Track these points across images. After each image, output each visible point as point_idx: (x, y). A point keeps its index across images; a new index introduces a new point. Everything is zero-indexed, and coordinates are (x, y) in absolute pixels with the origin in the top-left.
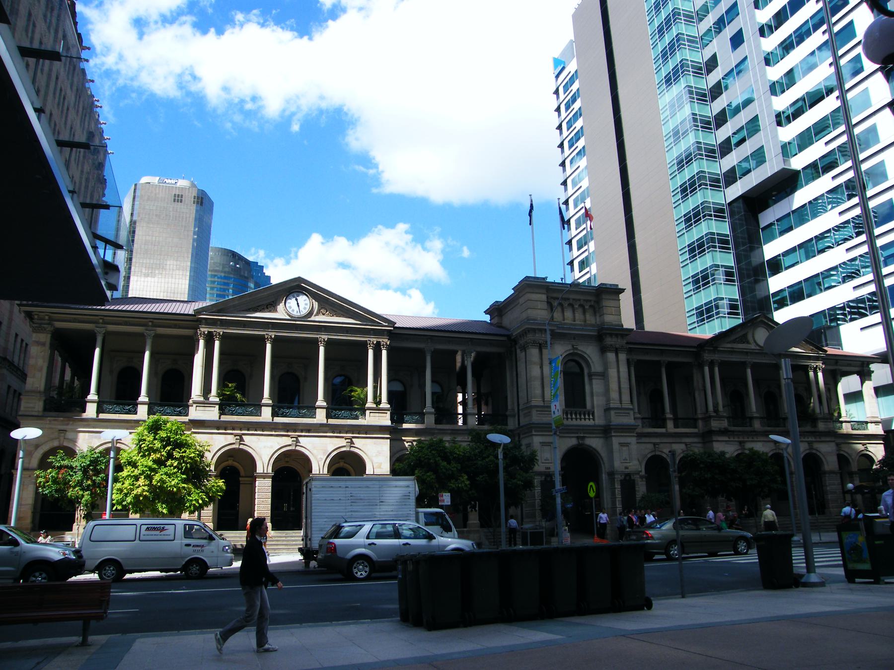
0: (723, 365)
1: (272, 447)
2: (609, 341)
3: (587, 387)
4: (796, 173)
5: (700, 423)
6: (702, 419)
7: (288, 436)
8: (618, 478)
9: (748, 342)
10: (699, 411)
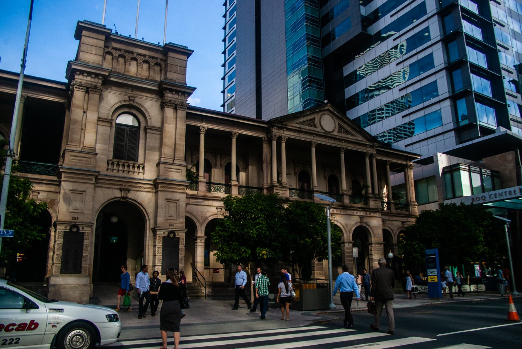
0: (290, 142)
2: (169, 96)
4: (370, 36)
6: (266, 189)
8: (160, 233)
9: (315, 126)
10: (265, 182)
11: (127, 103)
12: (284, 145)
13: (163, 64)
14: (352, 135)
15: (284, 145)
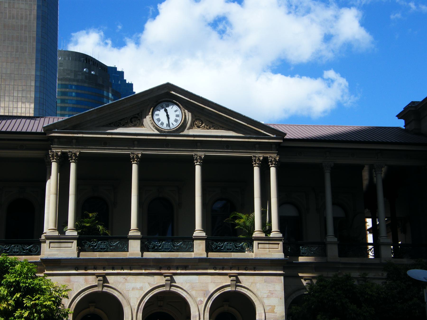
1: (141, 289)
7: (161, 274)
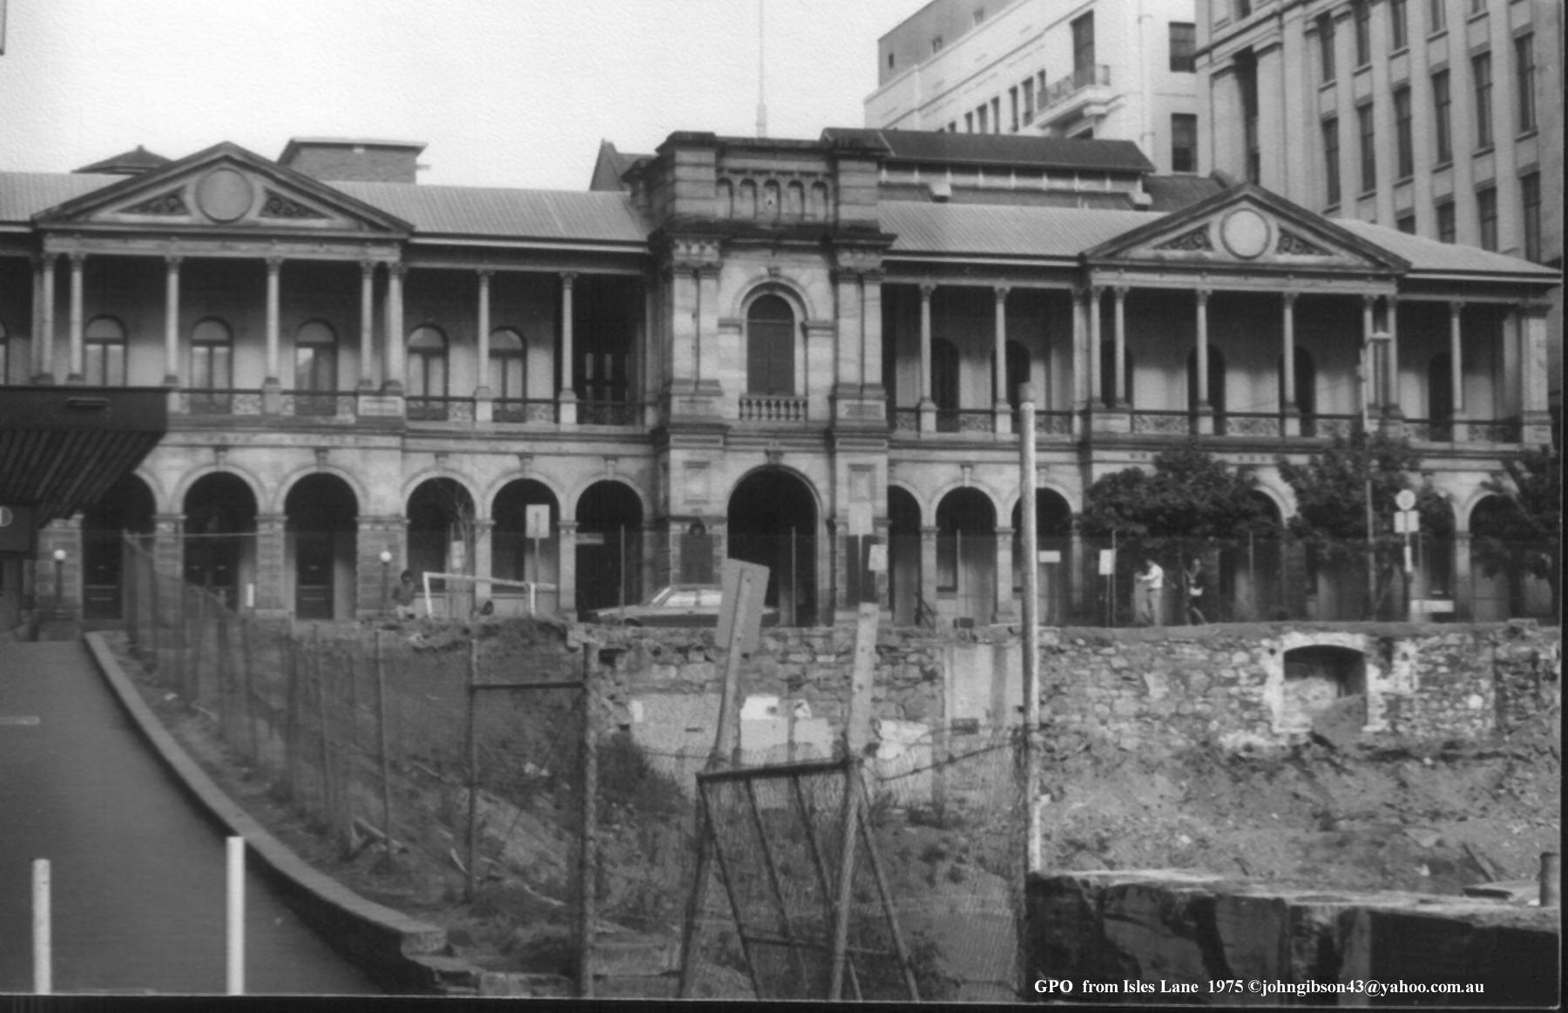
0: (1137, 298)
2: (846, 260)
3: (799, 352)
5: (1077, 422)
11: (766, 280)
12: (1119, 309)
13: (829, 183)
14: (1323, 252)
15: (1119, 309)
